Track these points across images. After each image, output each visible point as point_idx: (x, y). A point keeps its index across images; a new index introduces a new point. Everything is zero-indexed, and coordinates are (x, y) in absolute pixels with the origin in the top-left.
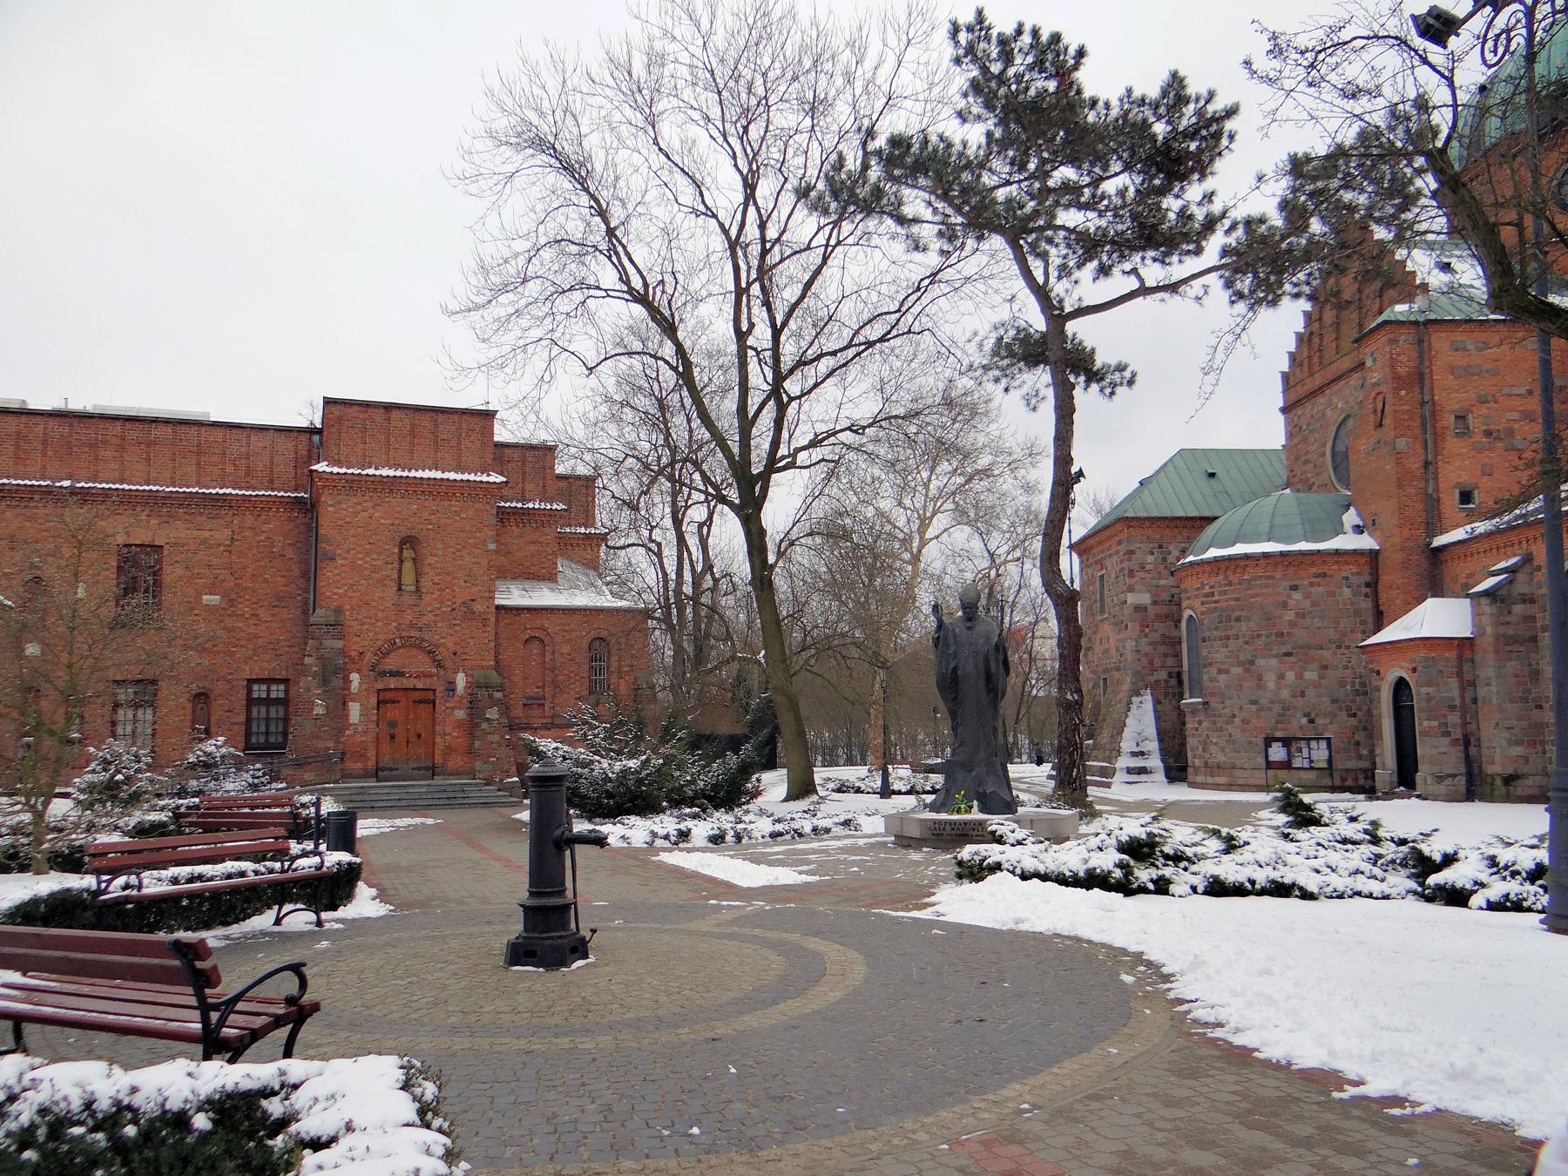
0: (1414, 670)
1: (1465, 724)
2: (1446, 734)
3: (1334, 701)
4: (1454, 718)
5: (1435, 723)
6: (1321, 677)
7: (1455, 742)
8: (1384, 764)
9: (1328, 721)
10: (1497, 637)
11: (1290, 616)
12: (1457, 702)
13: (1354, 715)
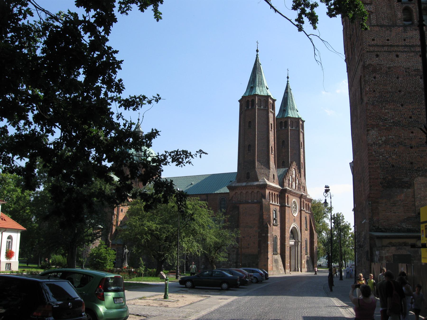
0: (117, 249)
2: (120, 258)
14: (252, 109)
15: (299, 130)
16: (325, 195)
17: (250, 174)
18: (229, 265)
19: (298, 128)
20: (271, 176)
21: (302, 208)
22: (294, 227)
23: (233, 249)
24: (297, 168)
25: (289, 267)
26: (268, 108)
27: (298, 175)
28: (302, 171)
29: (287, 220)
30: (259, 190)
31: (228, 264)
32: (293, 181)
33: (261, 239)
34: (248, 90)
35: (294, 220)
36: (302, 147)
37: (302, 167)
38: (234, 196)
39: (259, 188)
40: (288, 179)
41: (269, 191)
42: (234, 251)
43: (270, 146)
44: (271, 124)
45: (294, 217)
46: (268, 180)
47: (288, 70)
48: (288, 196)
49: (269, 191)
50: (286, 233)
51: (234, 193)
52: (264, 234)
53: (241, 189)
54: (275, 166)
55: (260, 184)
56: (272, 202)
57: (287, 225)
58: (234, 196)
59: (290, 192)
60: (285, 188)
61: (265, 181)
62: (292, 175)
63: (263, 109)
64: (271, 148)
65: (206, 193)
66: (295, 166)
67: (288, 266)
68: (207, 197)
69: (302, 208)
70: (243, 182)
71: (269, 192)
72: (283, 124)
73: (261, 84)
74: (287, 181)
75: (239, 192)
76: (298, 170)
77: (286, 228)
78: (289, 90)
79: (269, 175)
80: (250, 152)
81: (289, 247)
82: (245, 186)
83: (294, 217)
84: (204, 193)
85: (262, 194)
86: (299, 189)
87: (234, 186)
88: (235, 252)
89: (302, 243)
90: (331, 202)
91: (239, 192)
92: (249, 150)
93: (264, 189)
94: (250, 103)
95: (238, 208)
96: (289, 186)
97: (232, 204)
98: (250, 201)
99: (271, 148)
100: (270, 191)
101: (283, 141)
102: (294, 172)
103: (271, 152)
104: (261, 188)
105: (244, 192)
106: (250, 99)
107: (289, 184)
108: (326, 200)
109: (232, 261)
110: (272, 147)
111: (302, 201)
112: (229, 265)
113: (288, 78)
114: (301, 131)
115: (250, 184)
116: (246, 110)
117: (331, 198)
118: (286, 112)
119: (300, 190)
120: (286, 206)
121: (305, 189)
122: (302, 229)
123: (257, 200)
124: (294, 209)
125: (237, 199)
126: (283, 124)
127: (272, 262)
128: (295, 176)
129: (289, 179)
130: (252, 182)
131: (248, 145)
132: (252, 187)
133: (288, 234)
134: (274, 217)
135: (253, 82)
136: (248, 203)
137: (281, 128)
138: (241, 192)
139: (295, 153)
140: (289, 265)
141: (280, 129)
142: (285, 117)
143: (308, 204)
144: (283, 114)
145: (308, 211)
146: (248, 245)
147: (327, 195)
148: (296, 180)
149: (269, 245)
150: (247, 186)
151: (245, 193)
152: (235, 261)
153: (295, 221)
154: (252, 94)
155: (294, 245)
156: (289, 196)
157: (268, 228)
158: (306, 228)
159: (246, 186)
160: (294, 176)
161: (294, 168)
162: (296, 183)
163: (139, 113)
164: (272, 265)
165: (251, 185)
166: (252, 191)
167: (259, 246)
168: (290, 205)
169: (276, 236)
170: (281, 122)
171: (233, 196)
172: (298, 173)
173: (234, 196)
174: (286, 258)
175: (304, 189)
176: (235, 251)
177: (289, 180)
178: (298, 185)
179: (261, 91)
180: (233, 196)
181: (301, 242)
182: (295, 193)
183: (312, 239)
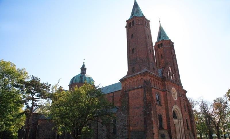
11: (49, 126)
21: (180, 95)
23: (125, 128)
28: (177, 72)
29: (169, 102)
32: (170, 74)
33: (145, 117)
35: (176, 104)
38: (125, 86)
42: (126, 129)
49: (150, 78)
51: (124, 84)
72: (160, 45)
85: (144, 80)
86: (176, 82)
92: (133, 52)
95: (128, 95)
98: (136, 88)
102: (170, 69)
104: (143, 75)
106: (131, 21)
110: (150, 49)
120: (166, 91)
126: (160, 45)
133: (171, 114)
134: (157, 98)
136: (135, 89)
137: (159, 48)
149: (153, 121)
151: (132, 82)
153: (176, 104)
160: (171, 71)
162: (173, 77)
163: (84, 59)
173: (125, 86)
174: (172, 133)
177: (167, 73)
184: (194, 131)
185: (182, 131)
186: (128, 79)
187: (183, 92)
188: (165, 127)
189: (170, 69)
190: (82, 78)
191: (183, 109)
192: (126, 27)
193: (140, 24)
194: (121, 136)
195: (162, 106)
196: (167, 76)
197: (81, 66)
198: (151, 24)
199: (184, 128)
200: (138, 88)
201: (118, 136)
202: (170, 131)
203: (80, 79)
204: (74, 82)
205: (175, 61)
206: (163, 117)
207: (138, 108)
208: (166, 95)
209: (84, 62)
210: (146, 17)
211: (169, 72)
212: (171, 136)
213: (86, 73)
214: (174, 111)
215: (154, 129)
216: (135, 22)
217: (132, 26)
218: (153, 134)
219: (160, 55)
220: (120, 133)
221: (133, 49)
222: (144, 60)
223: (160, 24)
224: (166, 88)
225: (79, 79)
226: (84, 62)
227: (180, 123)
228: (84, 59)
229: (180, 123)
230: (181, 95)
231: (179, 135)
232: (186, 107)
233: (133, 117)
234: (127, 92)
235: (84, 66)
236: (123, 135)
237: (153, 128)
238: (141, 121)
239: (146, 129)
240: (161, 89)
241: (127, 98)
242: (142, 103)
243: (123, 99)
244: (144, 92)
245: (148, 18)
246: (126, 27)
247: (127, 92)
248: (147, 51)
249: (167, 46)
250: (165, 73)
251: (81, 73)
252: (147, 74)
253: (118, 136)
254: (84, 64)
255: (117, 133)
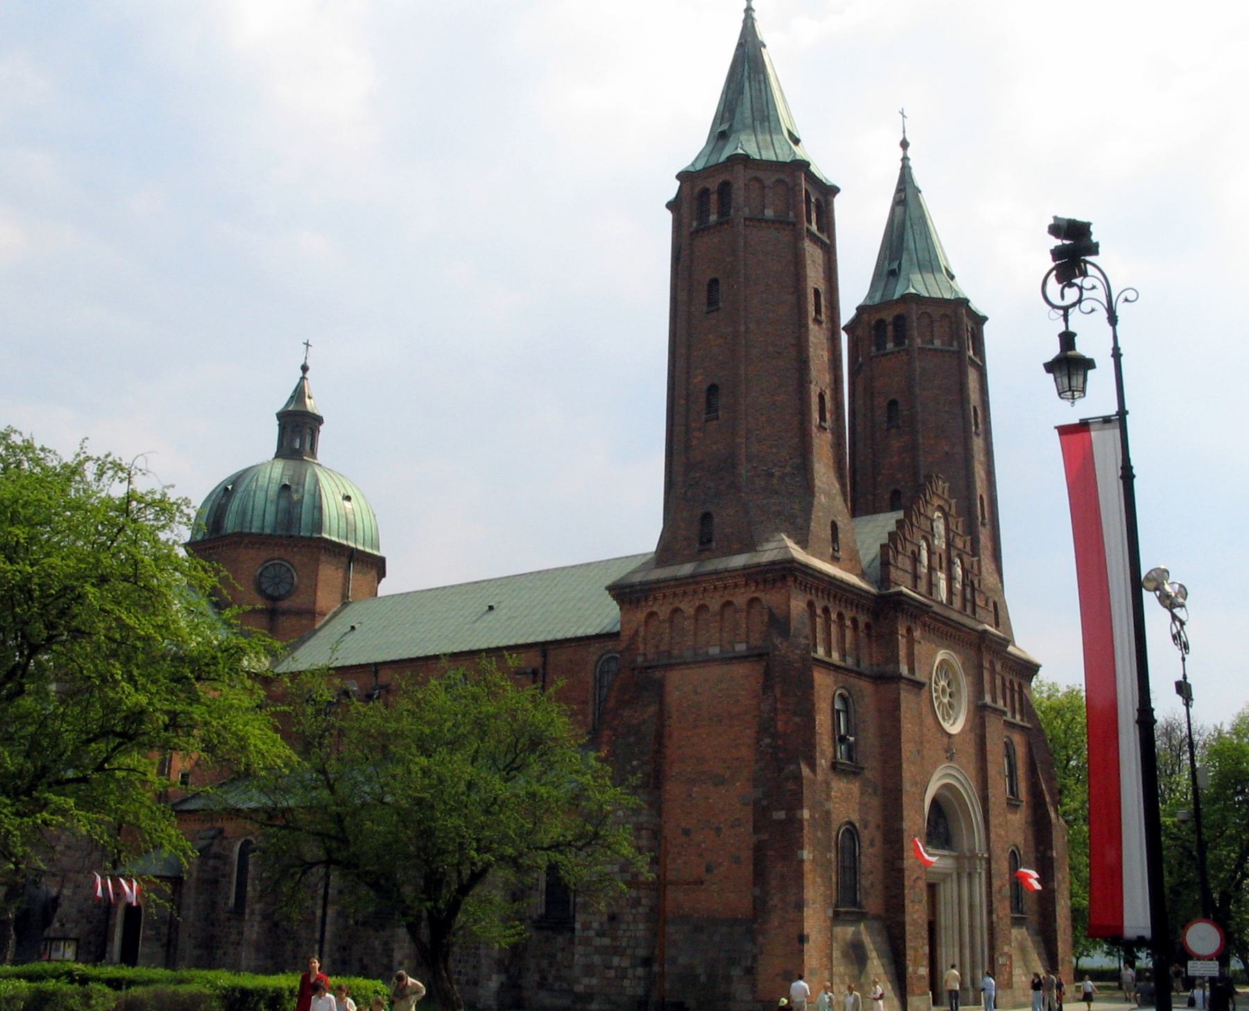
1: (170, 934)
2: (158, 940)
3: (80, 911)
4: (164, 930)
5: (153, 933)
6: (74, 893)
7: (163, 946)
8: (112, 959)
9: (73, 925)
10: (198, 879)
12: (168, 919)
13: (91, 922)
14: (721, 224)
15: (960, 354)
16: (1057, 301)
17: (716, 520)
18: (612, 973)
19: (955, 343)
20: (819, 528)
21: (988, 699)
22: (946, 786)
24: (953, 509)
25: (926, 982)
26: (797, 215)
27: (959, 543)
28: (984, 535)
29: (907, 748)
30: (756, 595)
31: (609, 968)
33: (766, 837)
34: (710, 148)
36: (977, 427)
37: (983, 518)
38: (642, 629)
39: (757, 584)
40: (909, 553)
41: (809, 597)
42: (636, 903)
43: (814, 391)
44: (817, 292)
45: (950, 736)
46: (803, 543)
47: (902, 113)
48: (909, 630)
50: (905, 813)
51: (641, 615)
52: (783, 812)
53: (675, 594)
54: (843, 486)
55: (759, 565)
56: (829, 653)
57: (908, 771)
58: (642, 634)
59: (919, 613)
60: (892, 590)
61: (787, 547)
62: (930, 537)
63: (773, 222)
64: (815, 400)
65: (541, 639)
66: (946, 496)
67: (922, 977)
68: (545, 655)
69: (988, 699)
70: (683, 562)
71: (811, 605)
73: (762, 122)
74: (904, 562)
75: (663, 610)
76: (961, 519)
77: (907, 786)
78: (909, 191)
79: (808, 519)
80: (717, 418)
81: (922, 884)
82: (692, 576)
83: (945, 740)
84: (531, 640)
85: (770, 609)
86: (969, 611)
87: (641, 583)
88: (641, 910)
89: (993, 866)
90: (1117, 354)
91: (663, 610)
92: (711, 408)
93: (779, 584)
94: (714, 197)
95: (660, 686)
96: (915, 586)
97: (634, 669)
98: (714, 651)
99: (815, 400)
100: (814, 598)
101: (893, 404)
102: (940, 527)
103: (816, 416)
104: (765, 581)
105: (688, 607)
106: (713, 184)
107: (916, 577)
108: (1067, 339)
109: (629, 951)
110: (821, 397)
111: (986, 664)
112: (612, 973)
113: (904, 144)
114: (970, 357)
115: (710, 566)
116: (694, 234)
117: (1113, 319)
118: (901, 279)
119: (974, 612)
120: (900, 677)
121: (1001, 613)
122: (992, 799)
123: (747, 642)
124: (945, 700)
125: (657, 647)
127: (830, 957)
128: (949, 544)
129: (913, 552)
130: (724, 555)
131: (705, 387)
132: (718, 580)
133: (915, 820)
135: (727, 115)
136: (709, 660)
137: (880, 345)
138: (676, 610)
139: (947, 453)
140: (924, 971)
141: (878, 349)
142: (898, 301)
143: (1020, 686)
144: (886, 285)
145: (1018, 717)
146: (709, 870)
147: (1072, 294)
148: (950, 563)
149: (807, 867)
150: (699, 579)
152: (641, 952)
153: (950, 759)
154: (723, 158)
155: (955, 876)
156: (917, 634)
157: (798, 778)
158: (1012, 792)
159: (693, 578)
160: (940, 543)
161: (940, 508)
162: (950, 579)
163: (307, 345)
164: (826, 974)
165: (716, 572)
166: (724, 600)
167: (760, 874)
168: (920, 676)
169: (850, 823)
170: (881, 324)
171: (637, 632)
172: (960, 531)
173: (642, 629)
174: (908, 936)
175: (998, 613)
176: (644, 901)
177: (916, 558)
178: (964, 585)
179: (761, 145)
180: (637, 632)
181: (989, 861)
182: (947, 621)
183: (1041, 848)
184: (1055, 931)
185: (972, 926)
186: (668, 592)
187: (1011, 670)
188: (873, 903)
189: (940, 527)
190: (296, 497)
191: (999, 789)
192: (670, 206)
193: (769, 213)
194: (606, 941)
195: (868, 774)
196: (916, 577)
197: (280, 402)
198: (841, 207)
199: (990, 912)
200: (731, 659)
201: (587, 942)
202: (902, 925)
203: (283, 503)
204: (230, 524)
205: (979, 457)
206: (865, 842)
207: (719, 781)
208: (897, 706)
209: (305, 369)
210: (812, 168)
211: (930, 552)
212: (905, 955)
213: (318, 455)
214: (935, 802)
215: (807, 912)
216: (739, 195)
217: (713, 218)
218: (802, 939)
219: (881, 402)
220: (595, 925)
221: (713, 390)
222: (776, 471)
223: (905, 159)
224: (898, 662)
225: (271, 509)
226: (305, 369)
227: (970, 875)
228: (307, 345)
229: (970, 875)
230: (994, 700)
231: (957, 950)
232: (1021, 772)
233: (686, 832)
234: (658, 675)
235: (299, 394)
236: (614, 938)
237: (800, 906)
238: (737, 860)
239: (760, 908)
240: (865, 665)
241: (652, 709)
242: (745, 752)
243: (626, 713)
244: (767, 687)
245: (824, 169)
246: (670, 206)
247: (658, 675)
248: (804, 412)
249: (937, 343)
250: (900, 557)
251: (278, 455)
252: (790, 582)
253: (587, 942)
254: (303, 378)
255: (578, 926)
